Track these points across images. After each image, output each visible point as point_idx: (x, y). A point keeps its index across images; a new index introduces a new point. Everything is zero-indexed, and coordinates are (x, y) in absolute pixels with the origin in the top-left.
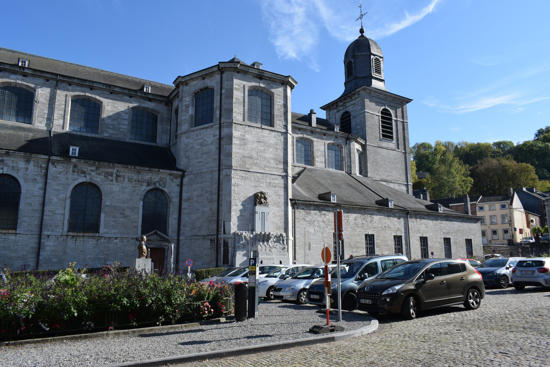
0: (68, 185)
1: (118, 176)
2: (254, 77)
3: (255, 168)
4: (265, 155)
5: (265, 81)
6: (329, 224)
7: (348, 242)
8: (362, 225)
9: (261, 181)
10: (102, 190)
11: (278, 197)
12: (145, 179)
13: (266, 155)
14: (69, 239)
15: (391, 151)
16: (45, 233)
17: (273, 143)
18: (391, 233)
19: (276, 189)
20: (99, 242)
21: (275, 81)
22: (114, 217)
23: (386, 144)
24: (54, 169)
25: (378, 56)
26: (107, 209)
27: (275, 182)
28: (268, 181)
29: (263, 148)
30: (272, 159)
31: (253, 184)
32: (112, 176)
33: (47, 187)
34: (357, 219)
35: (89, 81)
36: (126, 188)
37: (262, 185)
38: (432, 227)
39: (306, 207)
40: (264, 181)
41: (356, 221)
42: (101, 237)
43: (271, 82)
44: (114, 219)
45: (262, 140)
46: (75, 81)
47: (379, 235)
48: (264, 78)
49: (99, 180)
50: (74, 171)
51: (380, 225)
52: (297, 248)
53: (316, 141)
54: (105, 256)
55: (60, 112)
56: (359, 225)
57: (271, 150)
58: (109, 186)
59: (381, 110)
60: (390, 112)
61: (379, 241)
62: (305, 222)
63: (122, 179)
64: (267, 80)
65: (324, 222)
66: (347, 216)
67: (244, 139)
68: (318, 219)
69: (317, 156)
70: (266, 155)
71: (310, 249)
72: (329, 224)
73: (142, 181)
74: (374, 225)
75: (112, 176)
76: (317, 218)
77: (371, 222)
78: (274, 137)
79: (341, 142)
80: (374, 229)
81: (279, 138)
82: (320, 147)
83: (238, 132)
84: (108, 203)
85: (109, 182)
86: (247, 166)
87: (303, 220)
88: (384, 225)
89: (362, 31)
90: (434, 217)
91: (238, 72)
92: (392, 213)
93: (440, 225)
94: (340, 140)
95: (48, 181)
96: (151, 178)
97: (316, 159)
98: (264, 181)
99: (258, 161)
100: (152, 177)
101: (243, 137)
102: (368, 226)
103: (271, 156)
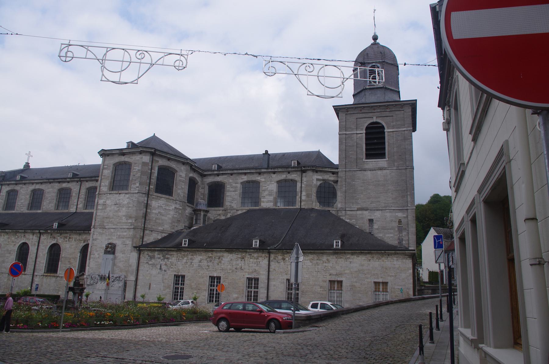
0: (47, 246)
1: (70, 238)
2: (119, 155)
3: (110, 225)
4: (119, 214)
5: (128, 155)
6: (172, 267)
7: (188, 284)
8: (208, 268)
9: (113, 234)
10: (61, 248)
11: (125, 245)
12: (83, 238)
13: (120, 214)
14: (44, 277)
15: (379, 172)
16: (36, 274)
17: (126, 203)
18: (244, 275)
19: (124, 239)
20: (57, 279)
21: (134, 154)
22: (65, 264)
23: (373, 163)
24: (43, 237)
25: (372, 63)
26: (63, 259)
27: (124, 234)
28: (118, 234)
29: (118, 209)
30: (124, 216)
31: (107, 238)
32: (67, 238)
33: (39, 248)
34: (202, 261)
35: (94, 177)
36: (73, 245)
37: (113, 237)
38: (309, 267)
39: (151, 253)
40: (116, 234)
41: (200, 264)
42: (58, 276)
43: (132, 155)
44: (65, 265)
45: (118, 203)
46: (88, 179)
47: (227, 277)
48: (126, 153)
49: (61, 241)
50: (50, 238)
51: (229, 267)
52: (138, 287)
53: (263, 181)
54: (58, 288)
55: (81, 200)
56: (204, 268)
57: (124, 209)
58: (65, 245)
59: (366, 125)
60: (382, 124)
61: (227, 284)
62: (148, 266)
63: (72, 239)
64: (128, 154)
65: (166, 265)
66: (191, 259)
67: (105, 205)
68: (161, 263)
69: (263, 197)
70: (120, 214)
71: (149, 289)
72: (172, 267)
73: (81, 240)
74: (222, 266)
75: (67, 238)
76: (160, 262)
77: (218, 264)
78: (128, 198)
79: (296, 177)
80: (221, 271)
81: (132, 198)
82: (267, 187)
83: (102, 200)
84: (63, 256)
85: (65, 242)
86: (105, 224)
87: (147, 264)
88: (235, 267)
89: (375, 38)
90: (315, 255)
91: (108, 156)
92: (247, 254)
93: (325, 264)
94: (294, 174)
95: (40, 244)
96: (86, 237)
97: (262, 200)
98: (116, 234)
99: (113, 220)
100: (87, 237)
101: (105, 203)
102: (214, 268)
103: (124, 214)
